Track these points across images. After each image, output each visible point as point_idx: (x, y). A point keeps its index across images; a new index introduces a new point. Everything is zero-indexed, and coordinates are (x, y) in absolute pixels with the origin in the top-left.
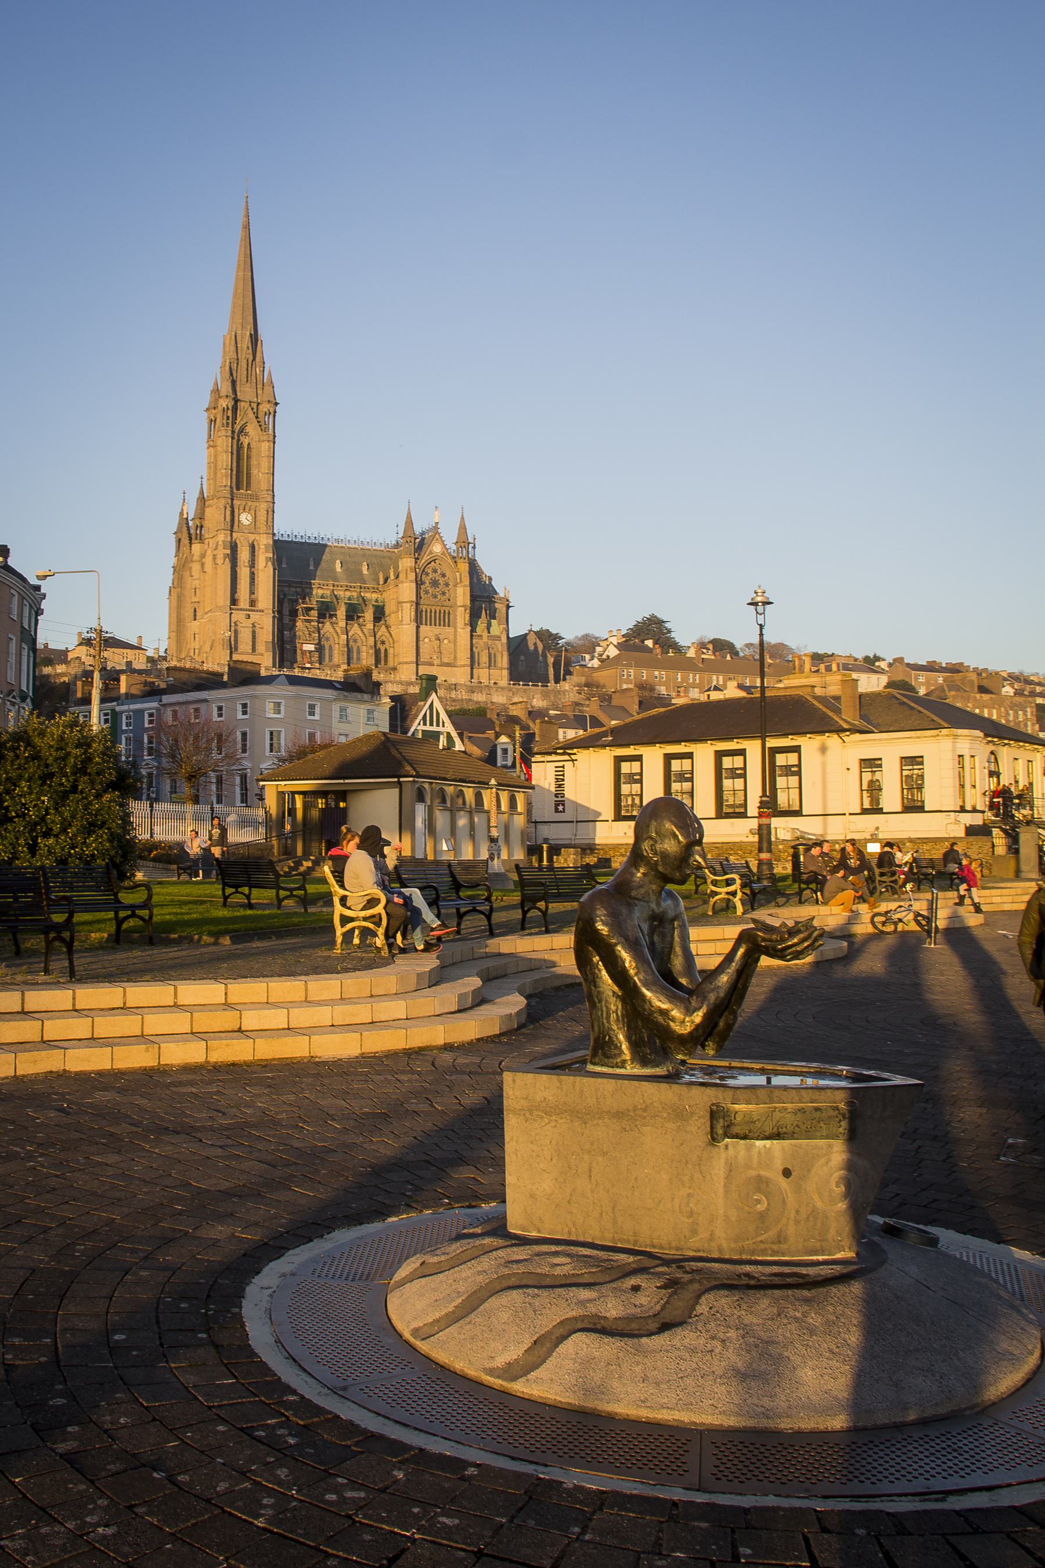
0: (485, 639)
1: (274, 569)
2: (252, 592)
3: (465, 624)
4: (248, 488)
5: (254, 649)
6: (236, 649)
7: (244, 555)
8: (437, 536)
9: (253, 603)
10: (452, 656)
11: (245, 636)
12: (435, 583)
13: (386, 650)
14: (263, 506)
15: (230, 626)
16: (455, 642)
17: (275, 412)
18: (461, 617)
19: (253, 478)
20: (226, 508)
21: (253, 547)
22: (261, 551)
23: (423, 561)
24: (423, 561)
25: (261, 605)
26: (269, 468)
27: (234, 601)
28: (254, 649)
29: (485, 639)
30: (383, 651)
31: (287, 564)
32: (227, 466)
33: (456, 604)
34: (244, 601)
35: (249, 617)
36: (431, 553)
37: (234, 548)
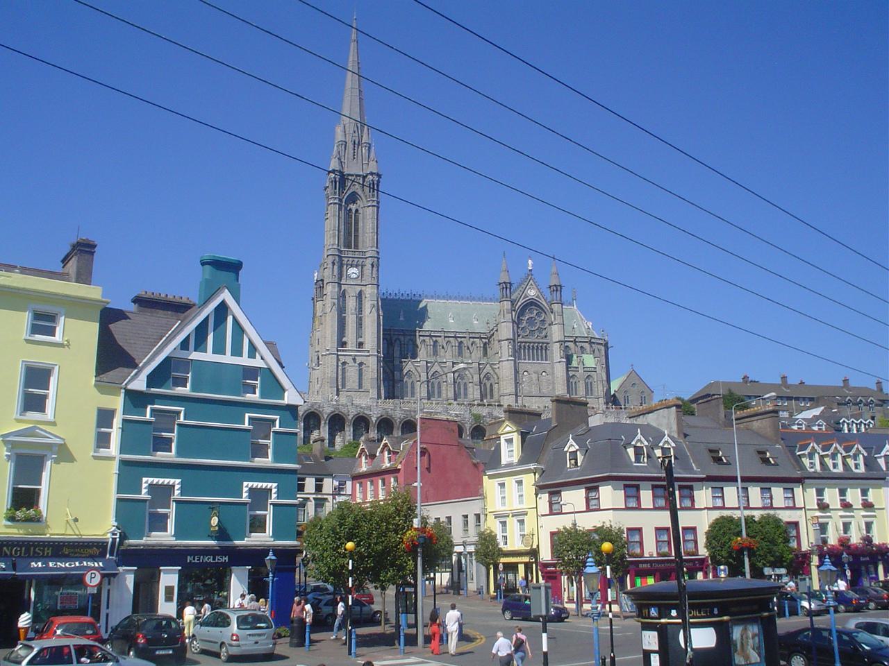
0: (581, 370)
1: (379, 315)
2: (359, 335)
3: (561, 358)
4: (356, 246)
5: (360, 386)
6: (343, 386)
7: (351, 303)
8: (531, 281)
9: (361, 345)
10: (551, 387)
11: (352, 373)
12: (531, 321)
13: (491, 385)
14: (369, 262)
15: (338, 366)
16: (553, 374)
17: (378, 182)
18: (556, 352)
19: (360, 239)
20: (333, 263)
21: (360, 296)
22: (367, 299)
23: (519, 304)
24: (519, 304)
25: (367, 347)
26: (373, 229)
27: (343, 344)
28: (360, 386)
29: (581, 370)
30: (488, 386)
31: (405, 317)
32: (335, 227)
33: (551, 340)
34: (351, 345)
35: (354, 360)
36: (526, 296)
37: (342, 296)
